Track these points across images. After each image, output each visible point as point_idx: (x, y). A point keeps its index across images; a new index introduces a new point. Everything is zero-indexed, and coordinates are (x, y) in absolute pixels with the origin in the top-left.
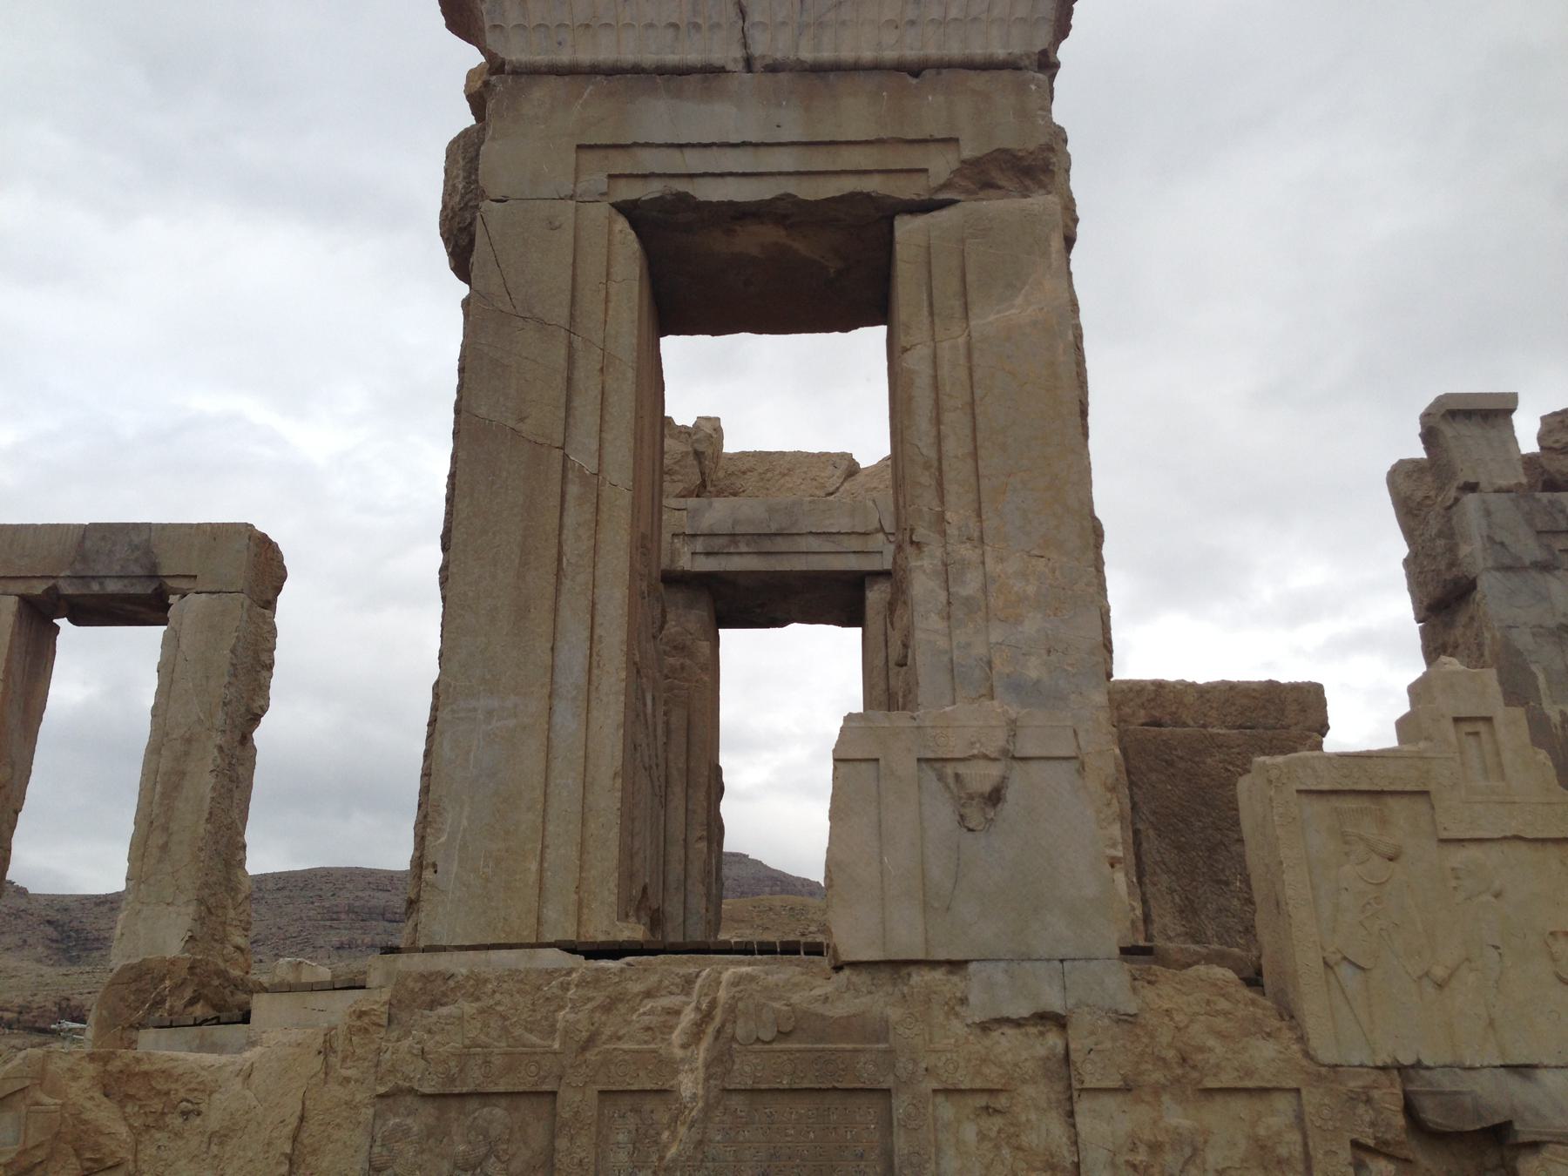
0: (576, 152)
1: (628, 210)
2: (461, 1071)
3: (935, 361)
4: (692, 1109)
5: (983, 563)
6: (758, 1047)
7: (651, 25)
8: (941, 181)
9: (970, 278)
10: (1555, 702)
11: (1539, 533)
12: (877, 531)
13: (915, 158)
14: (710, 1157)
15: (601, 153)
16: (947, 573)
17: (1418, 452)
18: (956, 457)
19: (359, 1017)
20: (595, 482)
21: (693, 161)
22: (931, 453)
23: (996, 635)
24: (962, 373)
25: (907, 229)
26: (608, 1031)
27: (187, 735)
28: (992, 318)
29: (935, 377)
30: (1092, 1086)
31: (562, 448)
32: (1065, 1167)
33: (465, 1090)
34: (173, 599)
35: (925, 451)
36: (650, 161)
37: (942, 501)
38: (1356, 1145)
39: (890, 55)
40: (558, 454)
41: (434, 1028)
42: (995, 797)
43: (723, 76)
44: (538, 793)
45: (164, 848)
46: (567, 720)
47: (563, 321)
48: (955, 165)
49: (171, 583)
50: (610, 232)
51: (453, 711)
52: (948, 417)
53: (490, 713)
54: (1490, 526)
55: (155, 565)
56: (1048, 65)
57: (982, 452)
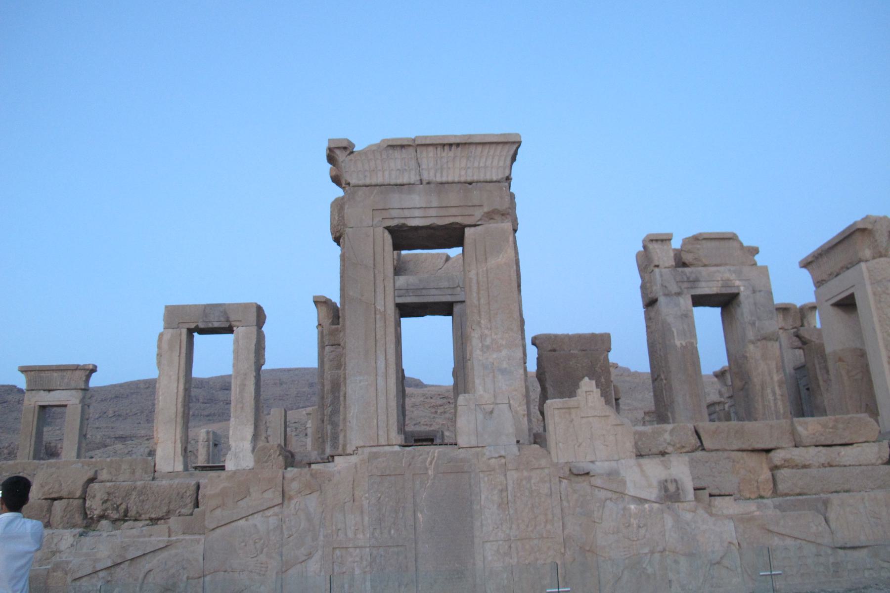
0: (372, 211)
1: (388, 228)
3: (477, 274)
5: (491, 335)
8: (478, 219)
10: (679, 341)
11: (677, 282)
12: (457, 287)
13: (469, 211)
15: (380, 211)
16: (482, 338)
17: (642, 249)
20: (384, 314)
21: (407, 213)
22: (476, 302)
23: (495, 356)
25: (468, 232)
31: (374, 304)
34: (235, 328)
36: (394, 213)
37: (480, 317)
38: (560, 477)
39: (463, 179)
40: (373, 306)
42: (491, 412)
43: (414, 185)
44: (375, 402)
46: (381, 381)
47: (372, 266)
48: (483, 214)
49: (233, 323)
50: (383, 237)
52: (482, 292)
54: (662, 280)
56: (508, 179)
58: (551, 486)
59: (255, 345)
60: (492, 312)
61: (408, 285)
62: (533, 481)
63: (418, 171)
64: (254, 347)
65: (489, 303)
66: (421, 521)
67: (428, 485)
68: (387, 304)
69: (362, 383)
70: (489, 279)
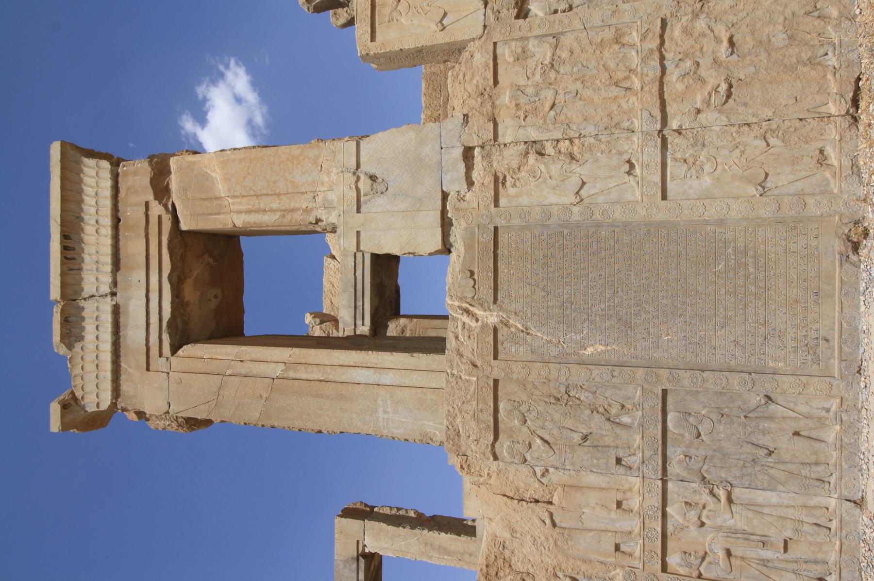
1: (174, 350)
2: (484, 423)
3: (239, 212)
4: (503, 317)
5: (324, 191)
6: (476, 287)
7: (97, 337)
9: (204, 196)
13: (154, 221)
14: (522, 309)
18: (279, 203)
19: (464, 469)
21: (154, 319)
22: (278, 214)
24: (245, 200)
25: (184, 227)
26: (470, 355)
27: (424, 545)
28: (220, 187)
29: (246, 212)
30: (492, 136)
31: (273, 379)
32: (527, 148)
33: (492, 421)
34: (367, 550)
35: (277, 217)
37: (298, 209)
41: (467, 435)
42: (373, 178)
44: (419, 390)
45: (470, 555)
46: (388, 378)
48: (157, 202)
49: (360, 551)
51: (384, 428)
52: (263, 206)
53: (385, 412)
55: (352, 558)
57: (277, 192)
58: (536, 37)
59: (389, 525)
60: (290, 190)
61: (350, 307)
62: (522, 81)
63: (100, 299)
64: (391, 526)
65: (279, 195)
66: (601, 348)
67: (520, 326)
68: (274, 359)
69: (389, 410)
70: (244, 193)
